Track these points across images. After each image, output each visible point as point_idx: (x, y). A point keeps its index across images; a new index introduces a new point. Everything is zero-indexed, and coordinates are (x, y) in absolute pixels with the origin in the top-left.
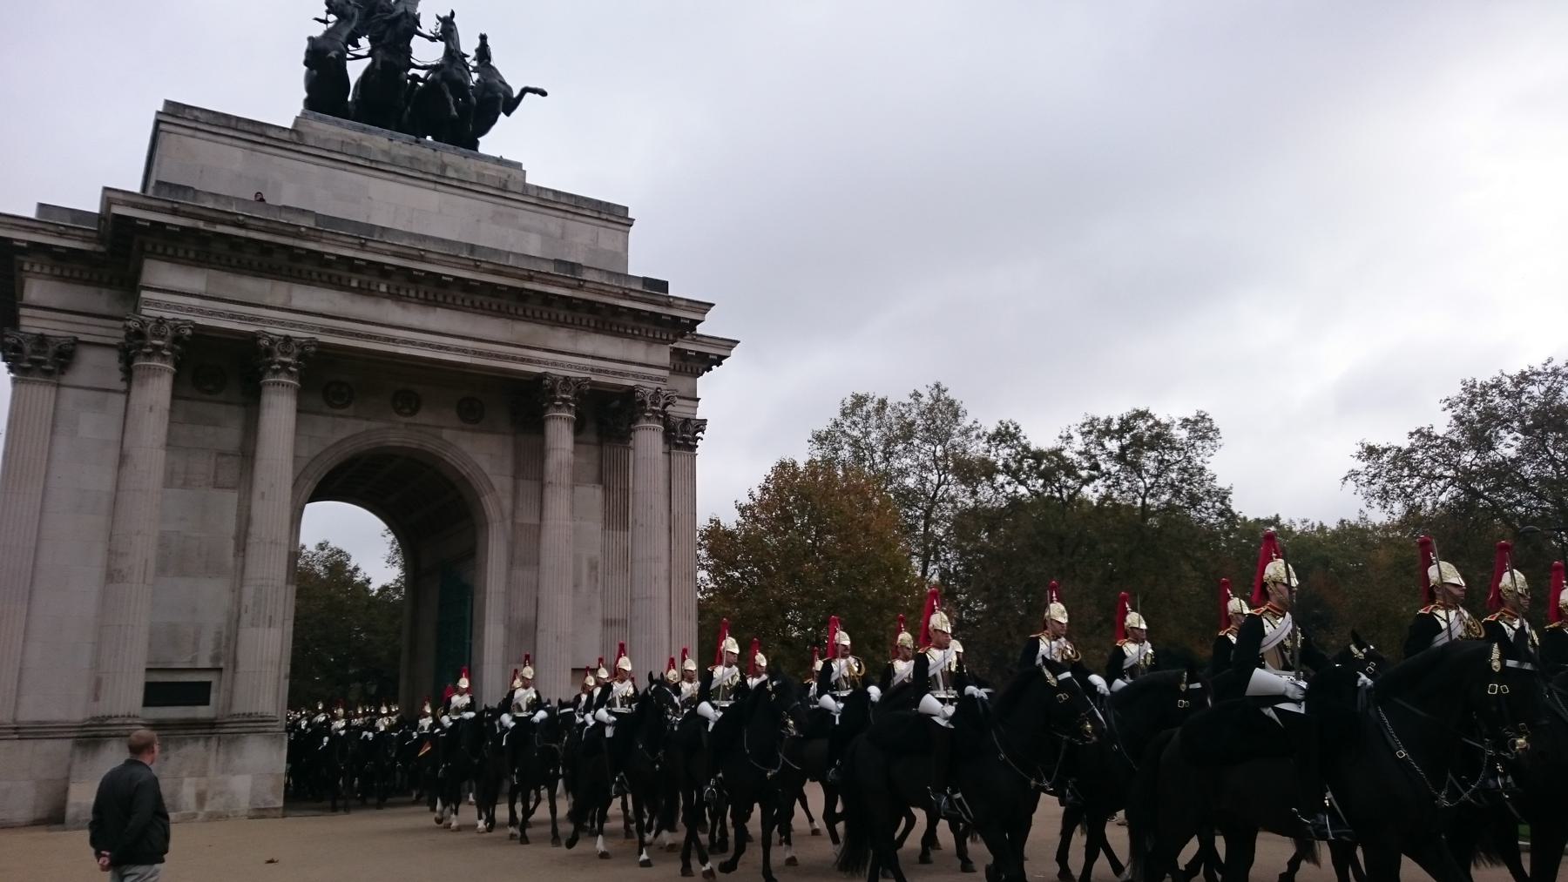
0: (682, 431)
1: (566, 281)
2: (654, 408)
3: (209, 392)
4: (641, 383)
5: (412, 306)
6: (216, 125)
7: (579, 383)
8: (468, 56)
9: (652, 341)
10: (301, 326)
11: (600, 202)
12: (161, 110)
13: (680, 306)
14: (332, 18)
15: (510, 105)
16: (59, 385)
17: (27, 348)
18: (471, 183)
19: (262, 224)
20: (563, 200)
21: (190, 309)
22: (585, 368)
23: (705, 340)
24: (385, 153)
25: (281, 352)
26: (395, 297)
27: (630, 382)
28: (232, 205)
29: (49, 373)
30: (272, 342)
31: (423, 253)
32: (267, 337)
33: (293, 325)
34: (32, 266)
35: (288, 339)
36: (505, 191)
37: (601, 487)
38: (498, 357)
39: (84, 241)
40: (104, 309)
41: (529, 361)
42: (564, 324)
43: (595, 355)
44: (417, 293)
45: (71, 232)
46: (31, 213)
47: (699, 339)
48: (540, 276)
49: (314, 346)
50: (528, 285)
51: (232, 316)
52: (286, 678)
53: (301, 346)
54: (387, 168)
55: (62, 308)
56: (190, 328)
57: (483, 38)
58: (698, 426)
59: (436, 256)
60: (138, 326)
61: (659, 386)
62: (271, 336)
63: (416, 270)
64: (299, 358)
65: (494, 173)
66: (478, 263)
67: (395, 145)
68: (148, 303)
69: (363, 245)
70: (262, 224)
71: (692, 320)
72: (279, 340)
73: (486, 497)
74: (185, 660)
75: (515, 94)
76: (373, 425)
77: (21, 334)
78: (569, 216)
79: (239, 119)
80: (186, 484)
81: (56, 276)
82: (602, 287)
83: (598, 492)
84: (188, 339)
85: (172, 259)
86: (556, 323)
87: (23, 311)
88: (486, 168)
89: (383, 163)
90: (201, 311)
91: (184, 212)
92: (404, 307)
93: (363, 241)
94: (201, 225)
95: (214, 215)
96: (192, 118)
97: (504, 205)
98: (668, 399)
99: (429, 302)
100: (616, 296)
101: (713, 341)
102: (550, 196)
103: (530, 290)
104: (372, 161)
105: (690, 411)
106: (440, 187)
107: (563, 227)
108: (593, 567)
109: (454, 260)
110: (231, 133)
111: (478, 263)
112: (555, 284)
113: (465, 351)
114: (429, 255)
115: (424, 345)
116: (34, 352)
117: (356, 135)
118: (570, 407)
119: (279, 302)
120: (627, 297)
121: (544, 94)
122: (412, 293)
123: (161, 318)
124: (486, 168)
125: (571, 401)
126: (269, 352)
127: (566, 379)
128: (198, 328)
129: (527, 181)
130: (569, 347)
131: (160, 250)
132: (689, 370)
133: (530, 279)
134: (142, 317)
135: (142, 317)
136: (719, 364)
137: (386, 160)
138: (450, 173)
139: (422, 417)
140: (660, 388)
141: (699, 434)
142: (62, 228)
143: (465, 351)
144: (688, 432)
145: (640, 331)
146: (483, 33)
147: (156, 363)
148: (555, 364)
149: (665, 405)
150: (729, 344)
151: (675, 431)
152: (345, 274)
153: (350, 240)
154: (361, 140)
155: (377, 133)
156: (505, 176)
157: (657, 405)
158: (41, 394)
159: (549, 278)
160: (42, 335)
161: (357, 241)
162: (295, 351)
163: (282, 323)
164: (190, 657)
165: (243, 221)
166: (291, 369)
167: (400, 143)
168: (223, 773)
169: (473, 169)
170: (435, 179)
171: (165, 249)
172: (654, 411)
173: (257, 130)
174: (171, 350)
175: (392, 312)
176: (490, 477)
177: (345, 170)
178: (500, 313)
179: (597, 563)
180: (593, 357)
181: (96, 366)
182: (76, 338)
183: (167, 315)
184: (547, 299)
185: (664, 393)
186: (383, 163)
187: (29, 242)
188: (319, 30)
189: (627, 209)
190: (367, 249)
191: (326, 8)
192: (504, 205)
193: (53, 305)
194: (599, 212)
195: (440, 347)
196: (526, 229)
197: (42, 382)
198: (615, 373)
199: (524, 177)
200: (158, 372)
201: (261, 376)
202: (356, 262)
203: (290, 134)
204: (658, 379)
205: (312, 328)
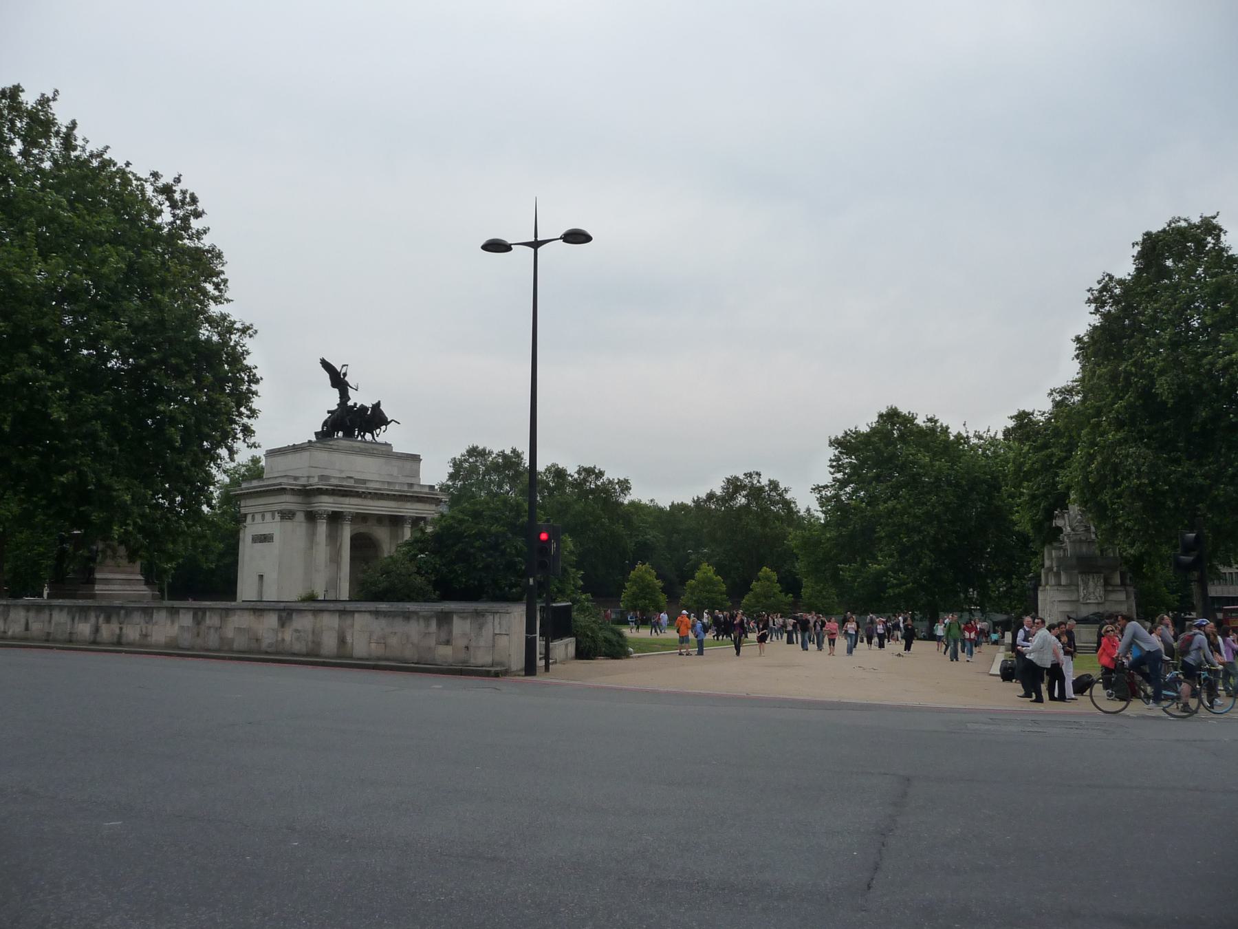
9: (432, 503)
10: (353, 509)
15: (386, 422)
20: (403, 456)
22: (413, 513)
24: (359, 447)
26: (372, 498)
29: (290, 519)
40: (300, 501)
51: (338, 507)
75: (389, 420)
99: (379, 499)
102: (399, 455)
117: (350, 443)
121: (399, 423)
128: (333, 512)
178: (394, 500)
181: (300, 517)
183: (326, 508)
184: (406, 496)
189: (419, 455)
195: (382, 511)
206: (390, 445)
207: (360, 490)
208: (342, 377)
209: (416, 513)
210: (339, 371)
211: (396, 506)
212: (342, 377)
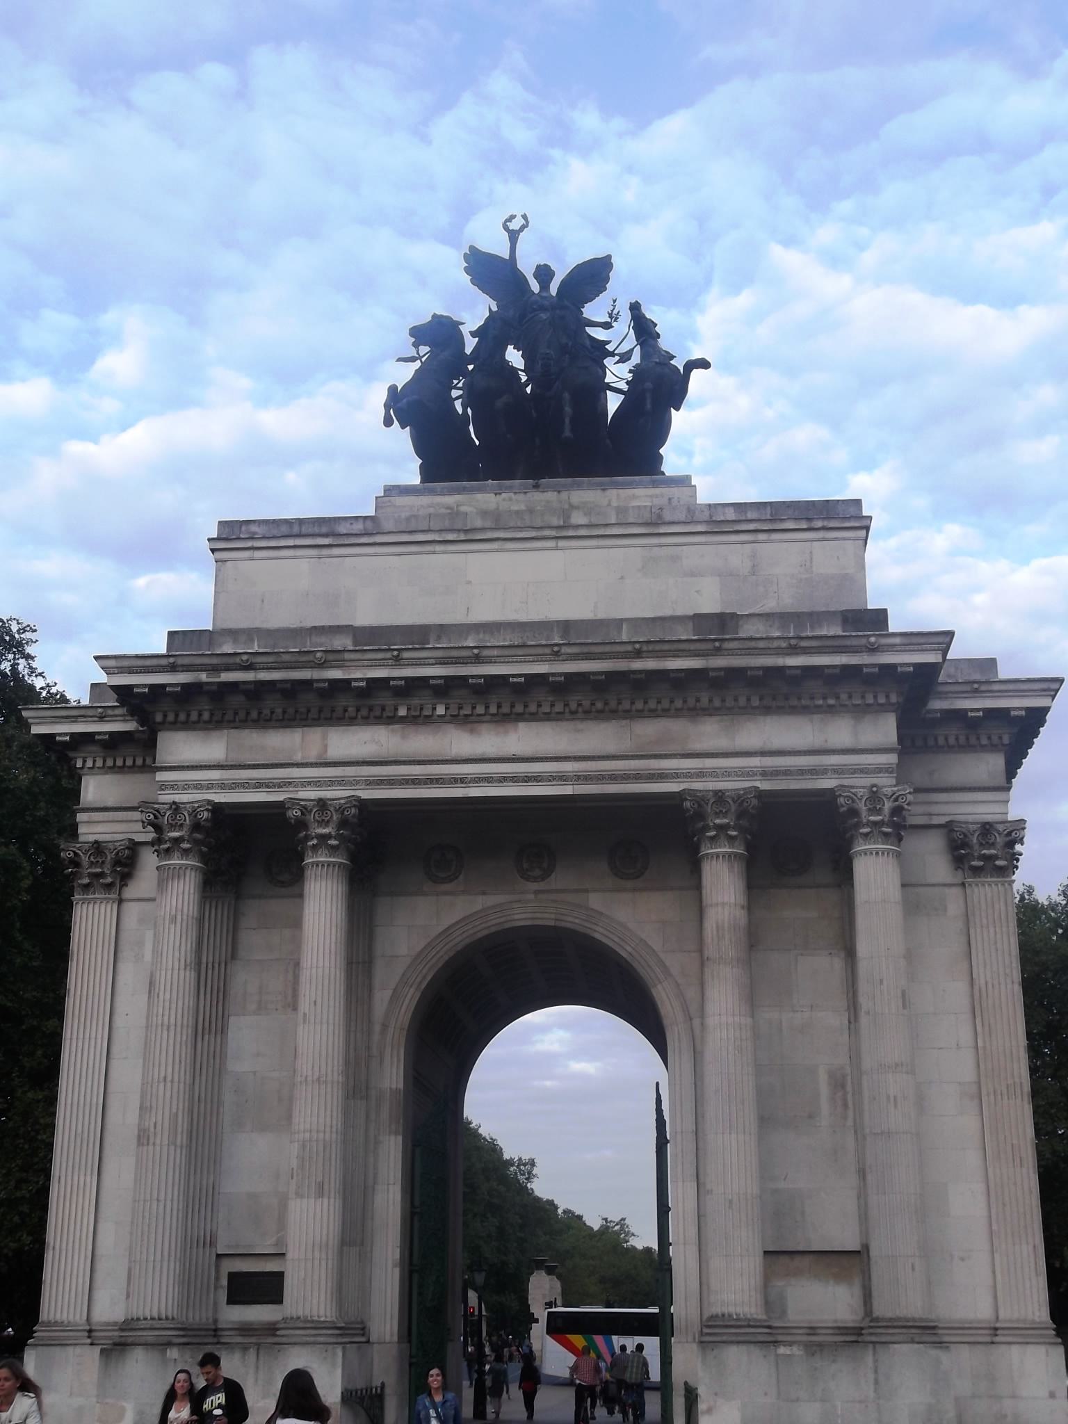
0: (981, 844)
1: (693, 647)
3: (283, 884)
4: (846, 782)
5: (484, 728)
6: (274, 537)
7: (740, 798)
8: (609, 342)
9: (862, 711)
11: (812, 504)
12: (215, 536)
13: (895, 645)
14: (424, 350)
16: (121, 901)
17: (85, 859)
18: (606, 525)
19: (271, 659)
20: (751, 515)
21: (210, 786)
23: (996, 687)
24: (484, 514)
25: (318, 822)
27: (827, 783)
28: (252, 640)
29: (109, 887)
30: (305, 810)
31: (476, 651)
32: (298, 804)
33: (331, 783)
34: (84, 762)
35: (322, 804)
36: (656, 524)
37: (843, 955)
38: (614, 778)
39: (124, 721)
41: (661, 776)
42: (709, 712)
43: (766, 749)
44: (487, 707)
45: (110, 712)
47: (983, 688)
48: (651, 647)
49: (355, 806)
50: (637, 665)
51: (259, 785)
52: (394, 1266)
53: (341, 810)
54: (489, 535)
55: (118, 805)
57: (635, 308)
58: (1009, 834)
59: (495, 652)
60: (152, 816)
61: (875, 781)
62: (302, 803)
63: (473, 677)
64: (343, 823)
65: (650, 504)
66: (556, 649)
67: (504, 500)
68: (163, 786)
69: (397, 658)
70: (271, 659)
71: (919, 667)
72: (314, 806)
73: (659, 986)
74: (269, 1243)
77: (78, 845)
78: (762, 537)
79: (301, 522)
80: (261, 1008)
81: (110, 768)
82: (753, 644)
83: (838, 963)
84: (209, 824)
85: (187, 726)
86: (696, 712)
87: (81, 817)
88: (634, 497)
89: (483, 529)
90: (223, 786)
91: (183, 666)
92: (472, 731)
93: (395, 653)
94: (203, 677)
95: (215, 661)
96: (247, 536)
97: (660, 545)
98: (896, 800)
99: (507, 718)
100: (779, 652)
101: (1011, 687)
102: (731, 515)
103: (640, 672)
104: (466, 531)
106: (562, 543)
107: (754, 556)
108: (838, 1083)
109: (520, 652)
110: (291, 542)
111: (556, 649)
112: (676, 654)
113: (562, 778)
114: (486, 653)
115: (503, 779)
116: (92, 864)
118: (731, 838)
119: (313, 755)
120: (799, 651)
121: (704, 364)
122: (480, 710)
123: (174, 803)
124: (634, 497)
125: (734, 828)
126: (302, 824)
127: (719, 796)
128: (217, 808)
129: (698, 502)
130: (722, 743)
131: (171, 717)
132: (984, 741)
133: (638, 654)
134: (156, 806)
135: (156, 806)
136: (1042, 722)
137: (488, 524)
138: (578, 518)
139: (557, 881)
140: (875, 786)
141: (1018, 847)
142: (100, 710)
143: (562, 778)
144: (993, 845)
145: (838, 698)
146: (633, 301)
147: (175, 861)
148: (701, 774)
149: (897, 811)
150: (1044, 686)
151: (965, 844)
152: (390, 702)
153: (380, 655)
154: (458, 506)
155: (480, 490)
156: (664, 501)
157: (879, 812)
159: (666, 647)
160: (96, 842)
161: (388, 655)
162: (335, 818)
164: (274, 1239)
165: (247, 660)
166: (333, 842)
167: (512, 495)
168: (264, 1398)
169: (615, 504)
170: (553, 533)
171: (177, 715)
172: (875, 824)
173: (324, 530)
174: (196, 842)
175: (459, 742)
176: (662, 956)
177: (434, 553)
179: (844, 1076)
180: (763, 754)
182: (130, 840)
185: (888, 791)
186: (483, 529)
187: (72, 735)
188: (404, 374)
189: (858, 503)
190: (402, 662)
191: (413, 340)
192: (660, 545)
193: (110, 804)
194: (809, 520)
196: (693, 575)
197: (105, 899)
198: (801, 772)
199: (694, 496)
200: (178, 872)
202: (392, 683)
203: (364, 523)
204: (879, 770)
205: (353, 782)
206: (688, 478)
207: (358, 675)
208: (535, 286)
209: (766, 774)
210: (506, 256)
211: (625, 746)
212: (535, 286)
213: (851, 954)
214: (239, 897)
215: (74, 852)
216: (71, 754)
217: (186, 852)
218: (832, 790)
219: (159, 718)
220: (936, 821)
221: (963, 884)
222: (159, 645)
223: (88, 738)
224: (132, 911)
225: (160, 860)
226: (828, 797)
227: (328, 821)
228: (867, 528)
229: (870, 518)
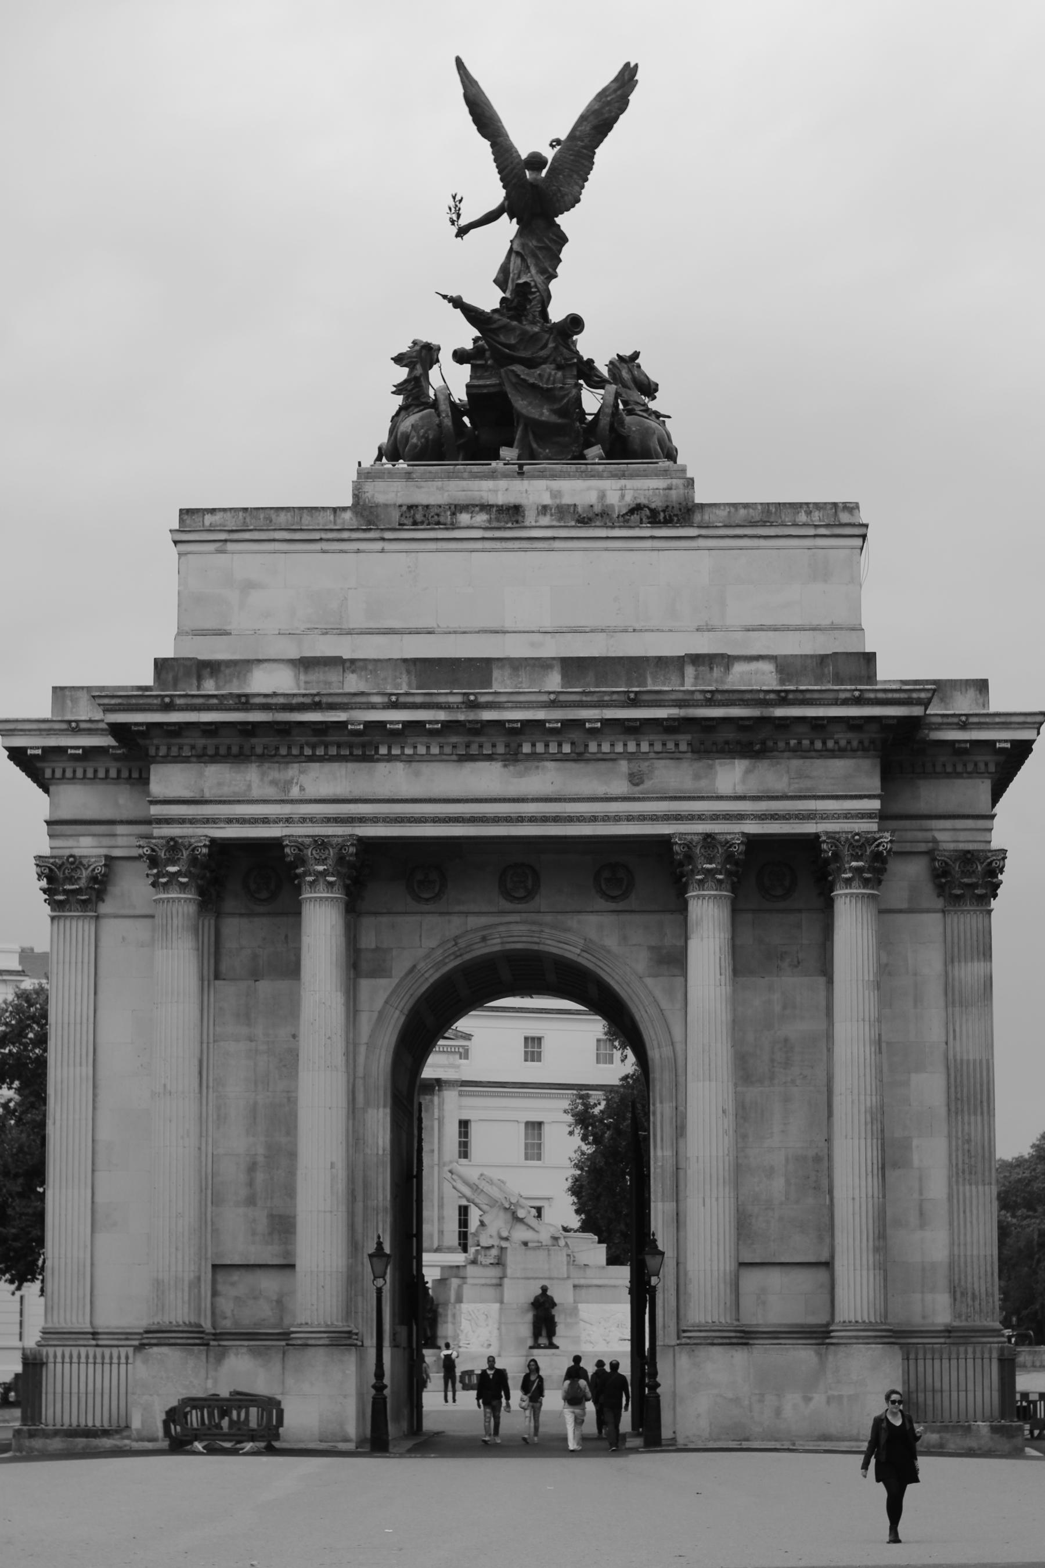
2: (854, 864)
12: (177, 527)
16: (97, 917)
30: (300, 847)
46: (42, 708)
56: (205, 846)
58: (991, 863)
64: (341, 859)
76: (473, 922)
105: (980, 836)
158: (81, 928)
163: (311, 820)
182: (108, 858)
187: (44, 749)
197: (79, 917)
201: (298, 890)
213: (830, 981)
214: (219, 915)
215: (49, 867)
216: (39, 765)
217: (183, 887)
218: (817, 836)
219: (152, 751)
220: (923, 847)
221: (943, 912)
222: (147, 678)
223: (61, 750)
224: (111, 928)
225: (158, 893)
226: (812, 841)
227: (326, 859)
228: (864, 537)
229: (866, 526)
